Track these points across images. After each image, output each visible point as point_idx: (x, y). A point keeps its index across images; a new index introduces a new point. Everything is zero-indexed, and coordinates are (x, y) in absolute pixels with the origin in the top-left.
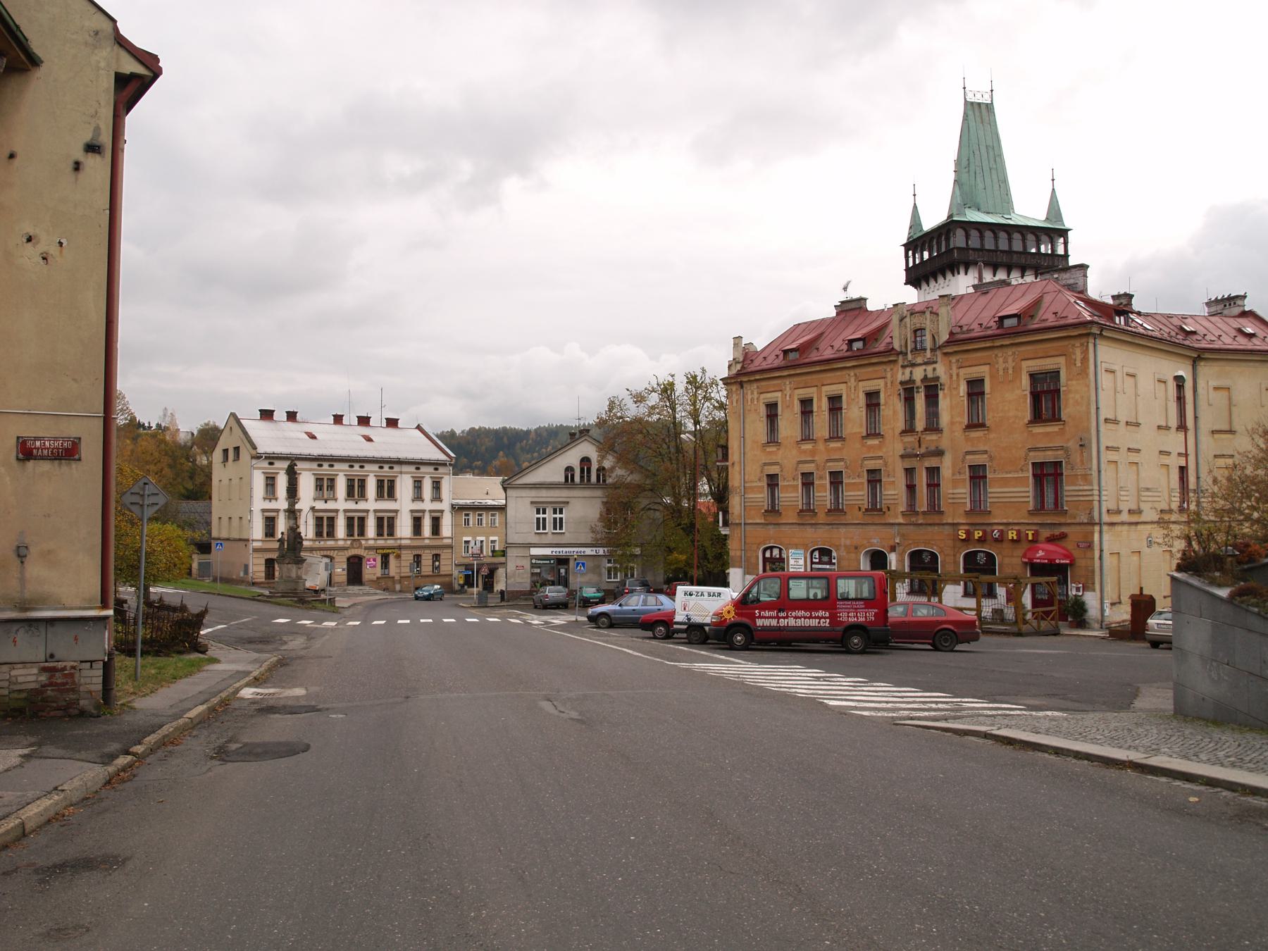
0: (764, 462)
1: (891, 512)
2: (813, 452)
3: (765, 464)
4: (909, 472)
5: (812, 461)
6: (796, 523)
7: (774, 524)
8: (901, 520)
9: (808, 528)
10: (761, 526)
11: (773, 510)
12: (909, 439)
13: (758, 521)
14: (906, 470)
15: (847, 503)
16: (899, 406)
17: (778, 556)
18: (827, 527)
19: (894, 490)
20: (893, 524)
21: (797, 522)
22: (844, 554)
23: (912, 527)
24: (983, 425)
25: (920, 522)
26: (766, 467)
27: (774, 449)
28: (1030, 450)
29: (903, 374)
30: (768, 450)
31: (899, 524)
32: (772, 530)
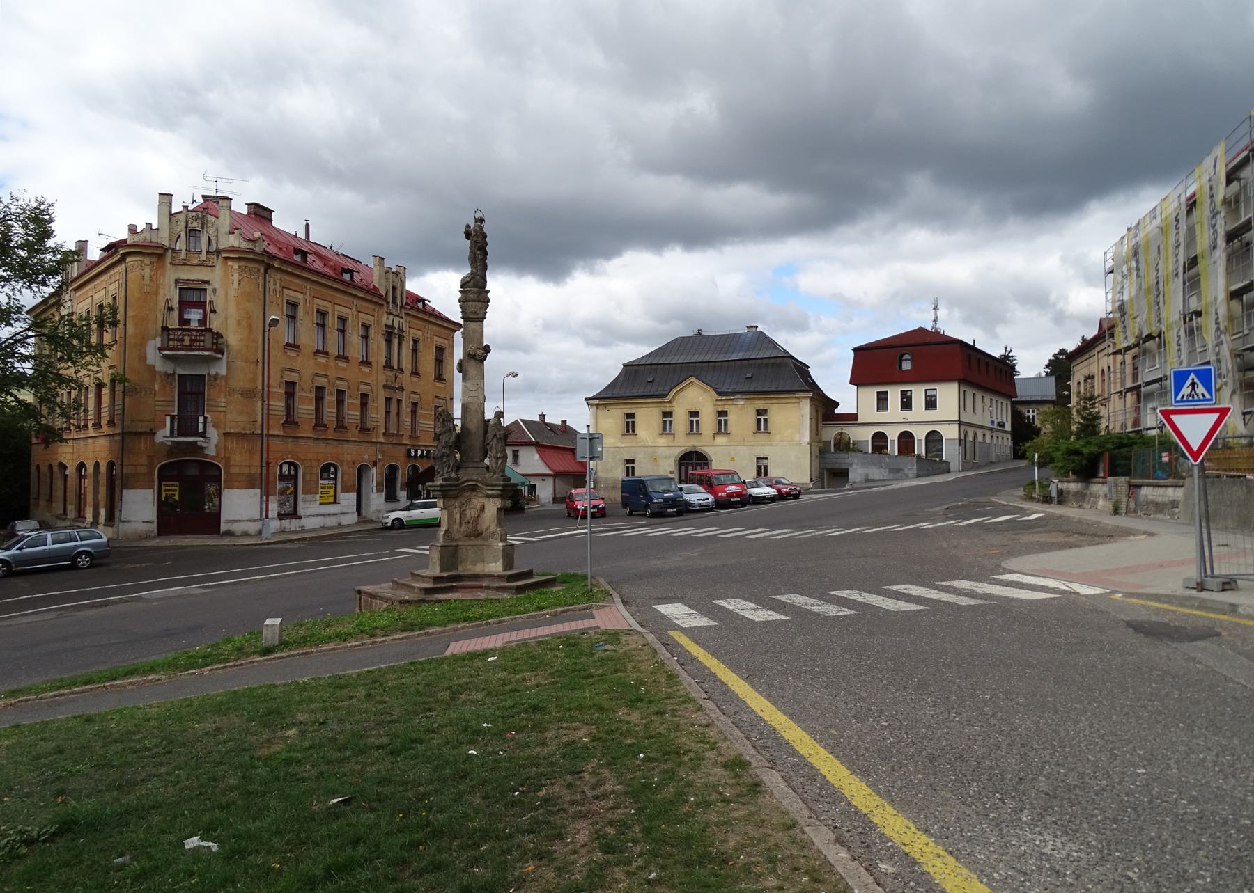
0: (284, 366)
1: (374, 433)
2: (326, 367)
3: (287, 369)
4: (388, 400)
5: (325, 376)
6: (311, 438)
7: (295, 438)
8: (383, 441)
9: (321, 442)
10: (280, 439)
11: (291, 421)
12: (390, 374)
13: (309, 435)
14: (386, 398)
15: (349, 421)
16: (383, 344)
17: (287, 473)
18: (335, 443)
19: (377, 414)
20: (376, 443)
21: (312, 436)
22: (345, 468)
23: (390, 446)
24: (418, 374)
25: (394, 442)
26: (286, 373)
27: (294, 354)
28: (436, 397)
29: (388, 318)
30: (290, 353)
31: (381, 443)
32: (290, 444)
